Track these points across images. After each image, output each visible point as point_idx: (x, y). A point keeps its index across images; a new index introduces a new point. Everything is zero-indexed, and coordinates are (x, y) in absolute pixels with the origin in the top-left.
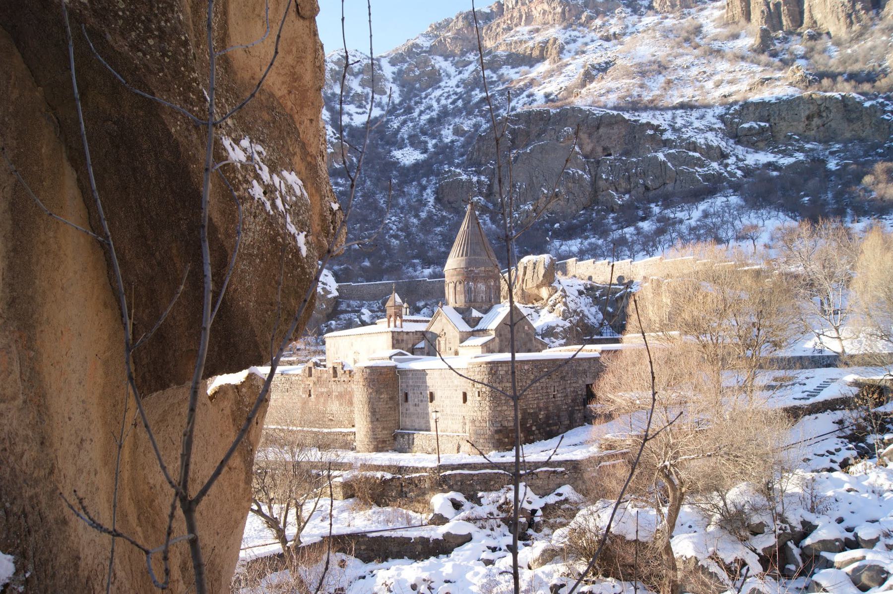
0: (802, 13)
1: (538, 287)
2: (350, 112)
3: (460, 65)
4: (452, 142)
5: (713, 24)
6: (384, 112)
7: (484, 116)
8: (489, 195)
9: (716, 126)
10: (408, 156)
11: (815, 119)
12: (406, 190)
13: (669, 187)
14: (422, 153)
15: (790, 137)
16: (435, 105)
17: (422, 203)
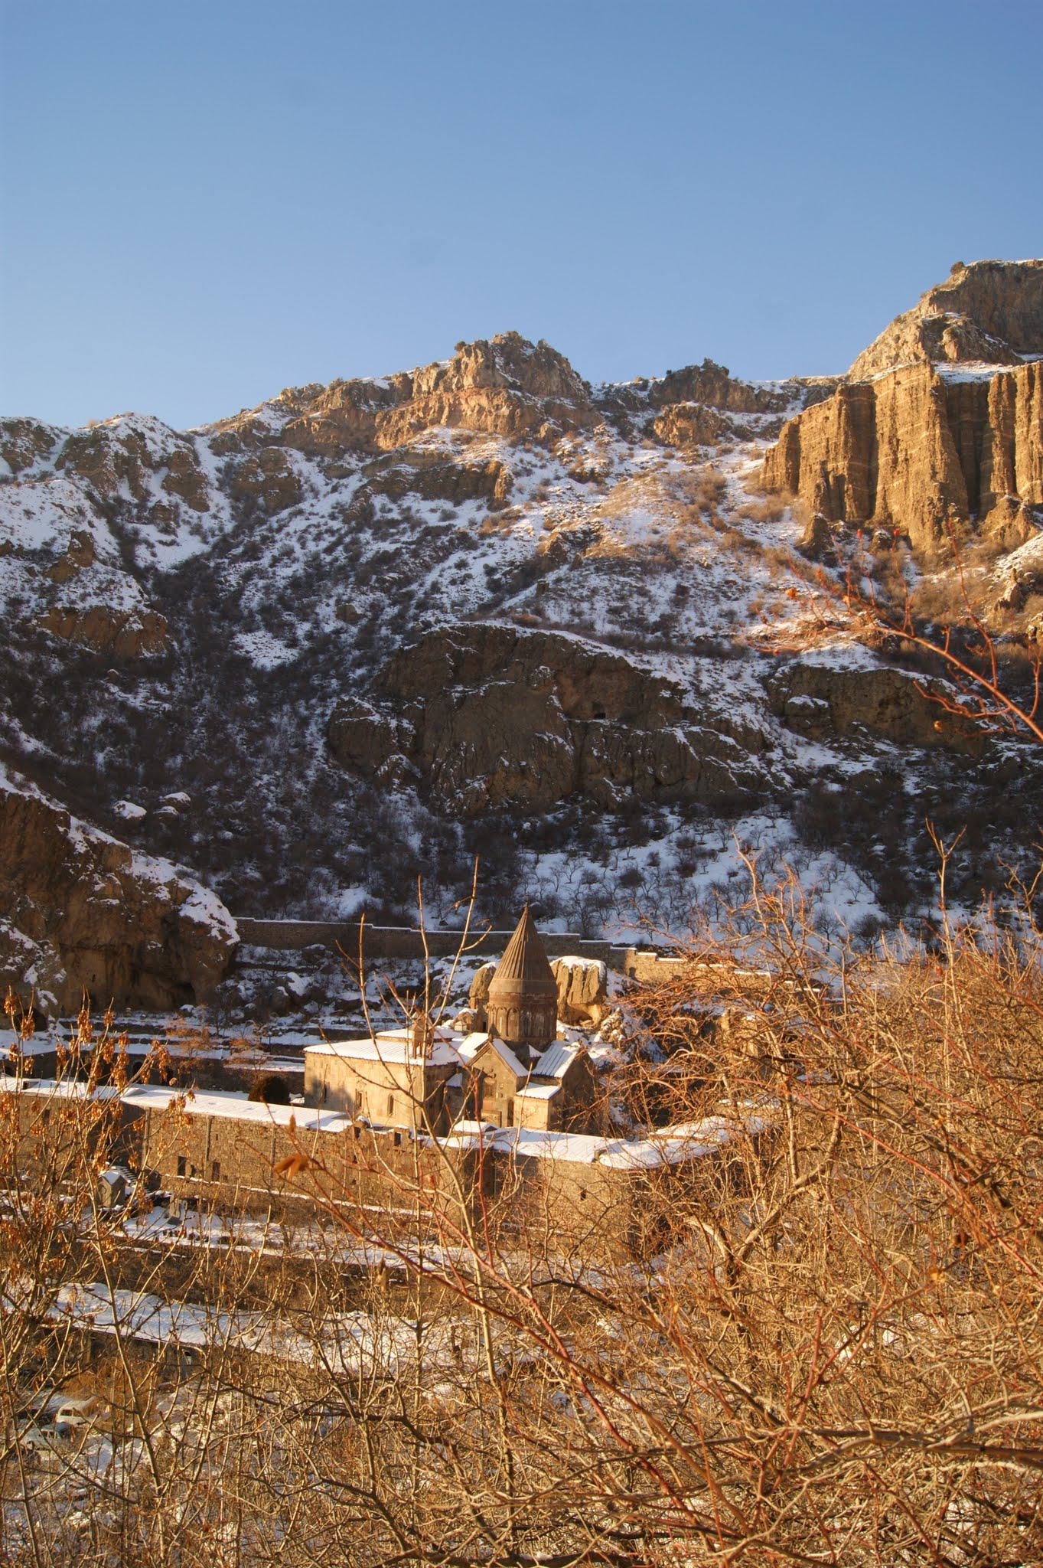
0: (872, 497)
1: (588, 1004)
2: (152, 540)
6: (207, 549)
8: (414, 754)
9: (756, 695)
10: (266, 651)
11: (891, 707)
12: (274, 720)
13: (690, 785)
14: (287, 646)
15: (856, 729)
16: (299, 552)
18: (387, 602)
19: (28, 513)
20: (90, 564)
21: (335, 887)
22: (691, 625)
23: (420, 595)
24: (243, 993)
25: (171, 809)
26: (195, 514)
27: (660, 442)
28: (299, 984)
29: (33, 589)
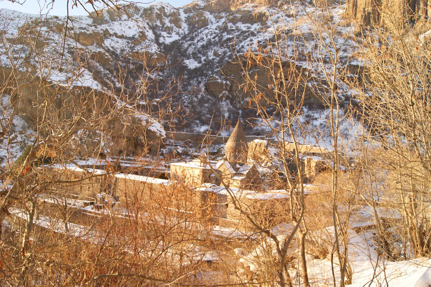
2: (164, 36)
3: (217, 18)
4: (213, 59)
5: (339, 16)
6: (180, 38)
7: (229, 48)
8: (230, 91)
10: (192, 64)
12: (191, 82)
16: (205, 38)
17: (199, 91)
18: (228, 51)
19: (129, 28)
20: (145, 40)
21: (199, 125)
22: (317, 55)
23: (238, 48)
24: (164, 152)
25: (155, 103)
26: (177, 29)
27: (314, 6)
28: (180, 150)
29: (128, 47)
